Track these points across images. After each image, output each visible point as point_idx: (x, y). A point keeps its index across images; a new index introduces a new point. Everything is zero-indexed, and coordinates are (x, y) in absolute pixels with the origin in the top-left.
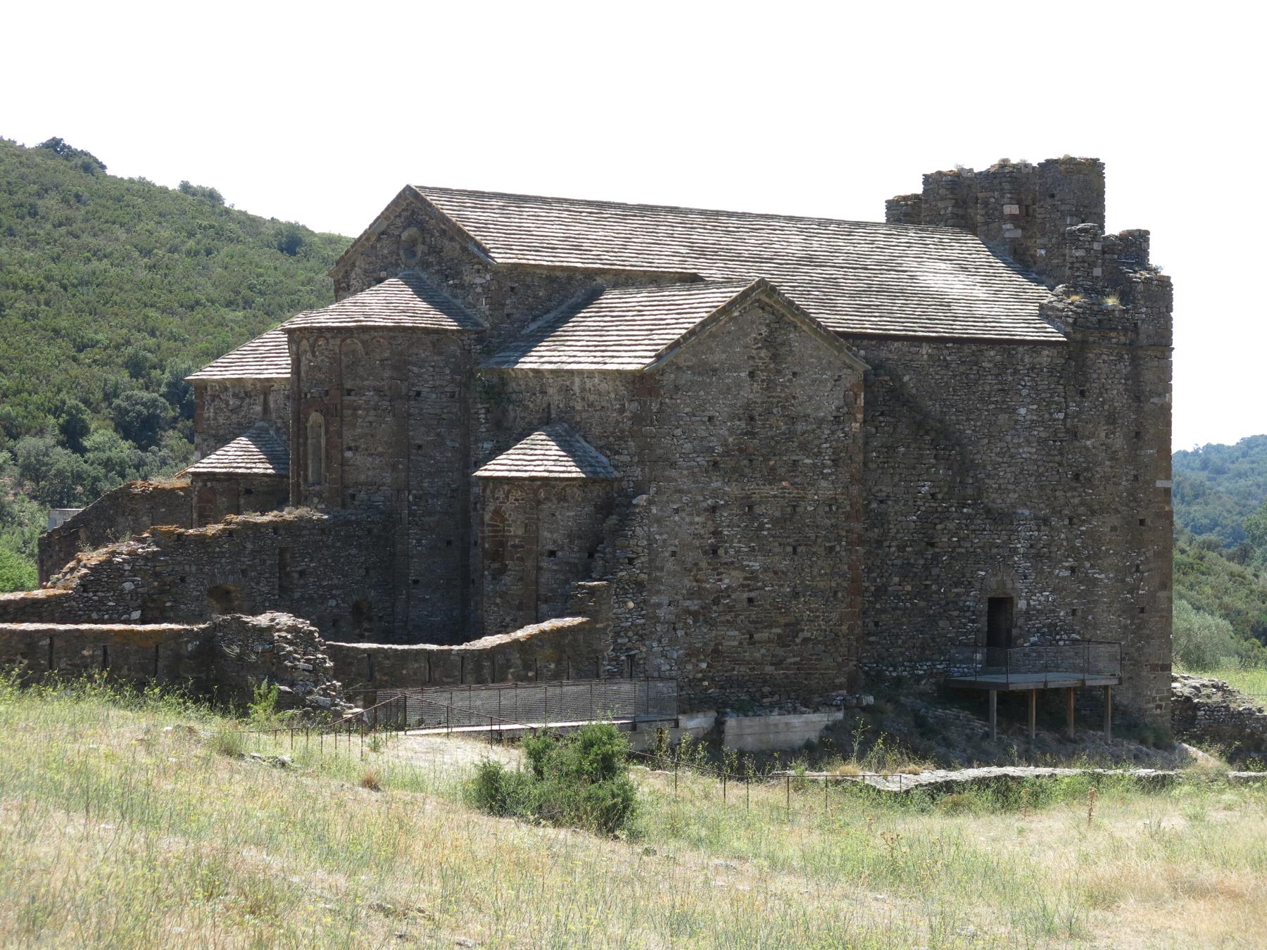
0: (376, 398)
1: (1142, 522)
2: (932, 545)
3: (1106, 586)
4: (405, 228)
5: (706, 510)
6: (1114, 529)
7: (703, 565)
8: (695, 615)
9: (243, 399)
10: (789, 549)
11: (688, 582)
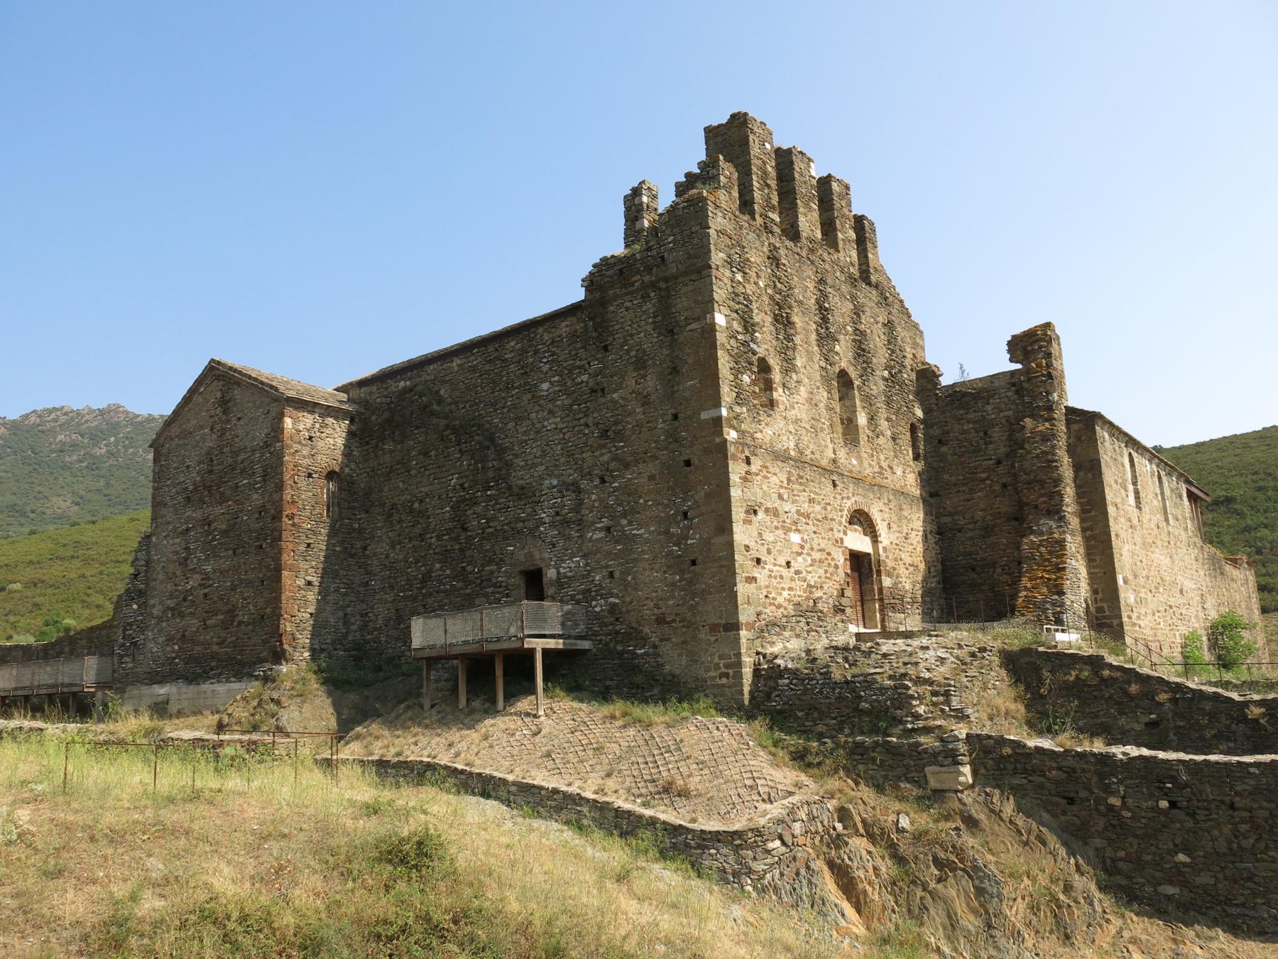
1: (688, 463)
2: (465, 530)
3: (647, 541)
5: (182, 533)
6: (652, 477)
7: (178, 573)
8: (172, 609)
10: (231, 552)
11: (170, 587)
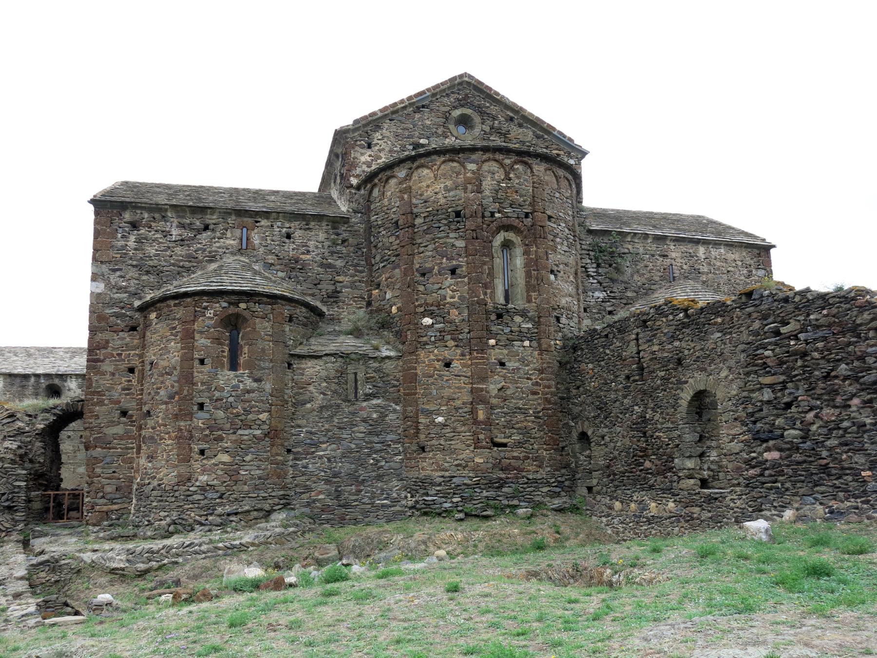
0: (566, 230)
4: (455, 108)
9: (199, 231)
